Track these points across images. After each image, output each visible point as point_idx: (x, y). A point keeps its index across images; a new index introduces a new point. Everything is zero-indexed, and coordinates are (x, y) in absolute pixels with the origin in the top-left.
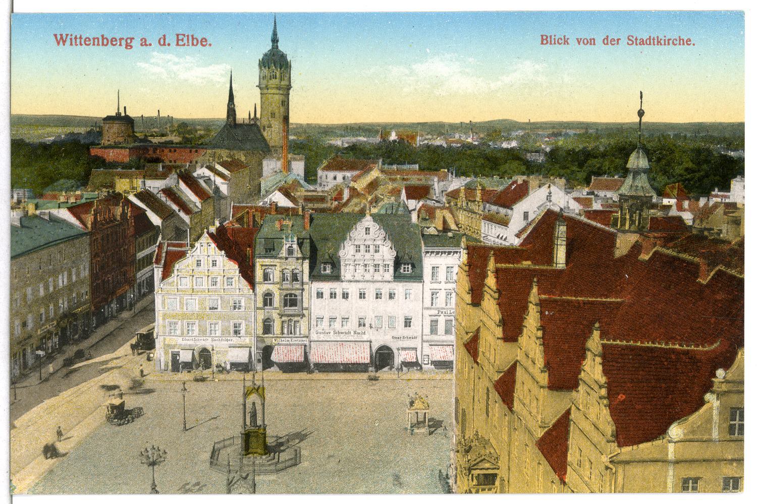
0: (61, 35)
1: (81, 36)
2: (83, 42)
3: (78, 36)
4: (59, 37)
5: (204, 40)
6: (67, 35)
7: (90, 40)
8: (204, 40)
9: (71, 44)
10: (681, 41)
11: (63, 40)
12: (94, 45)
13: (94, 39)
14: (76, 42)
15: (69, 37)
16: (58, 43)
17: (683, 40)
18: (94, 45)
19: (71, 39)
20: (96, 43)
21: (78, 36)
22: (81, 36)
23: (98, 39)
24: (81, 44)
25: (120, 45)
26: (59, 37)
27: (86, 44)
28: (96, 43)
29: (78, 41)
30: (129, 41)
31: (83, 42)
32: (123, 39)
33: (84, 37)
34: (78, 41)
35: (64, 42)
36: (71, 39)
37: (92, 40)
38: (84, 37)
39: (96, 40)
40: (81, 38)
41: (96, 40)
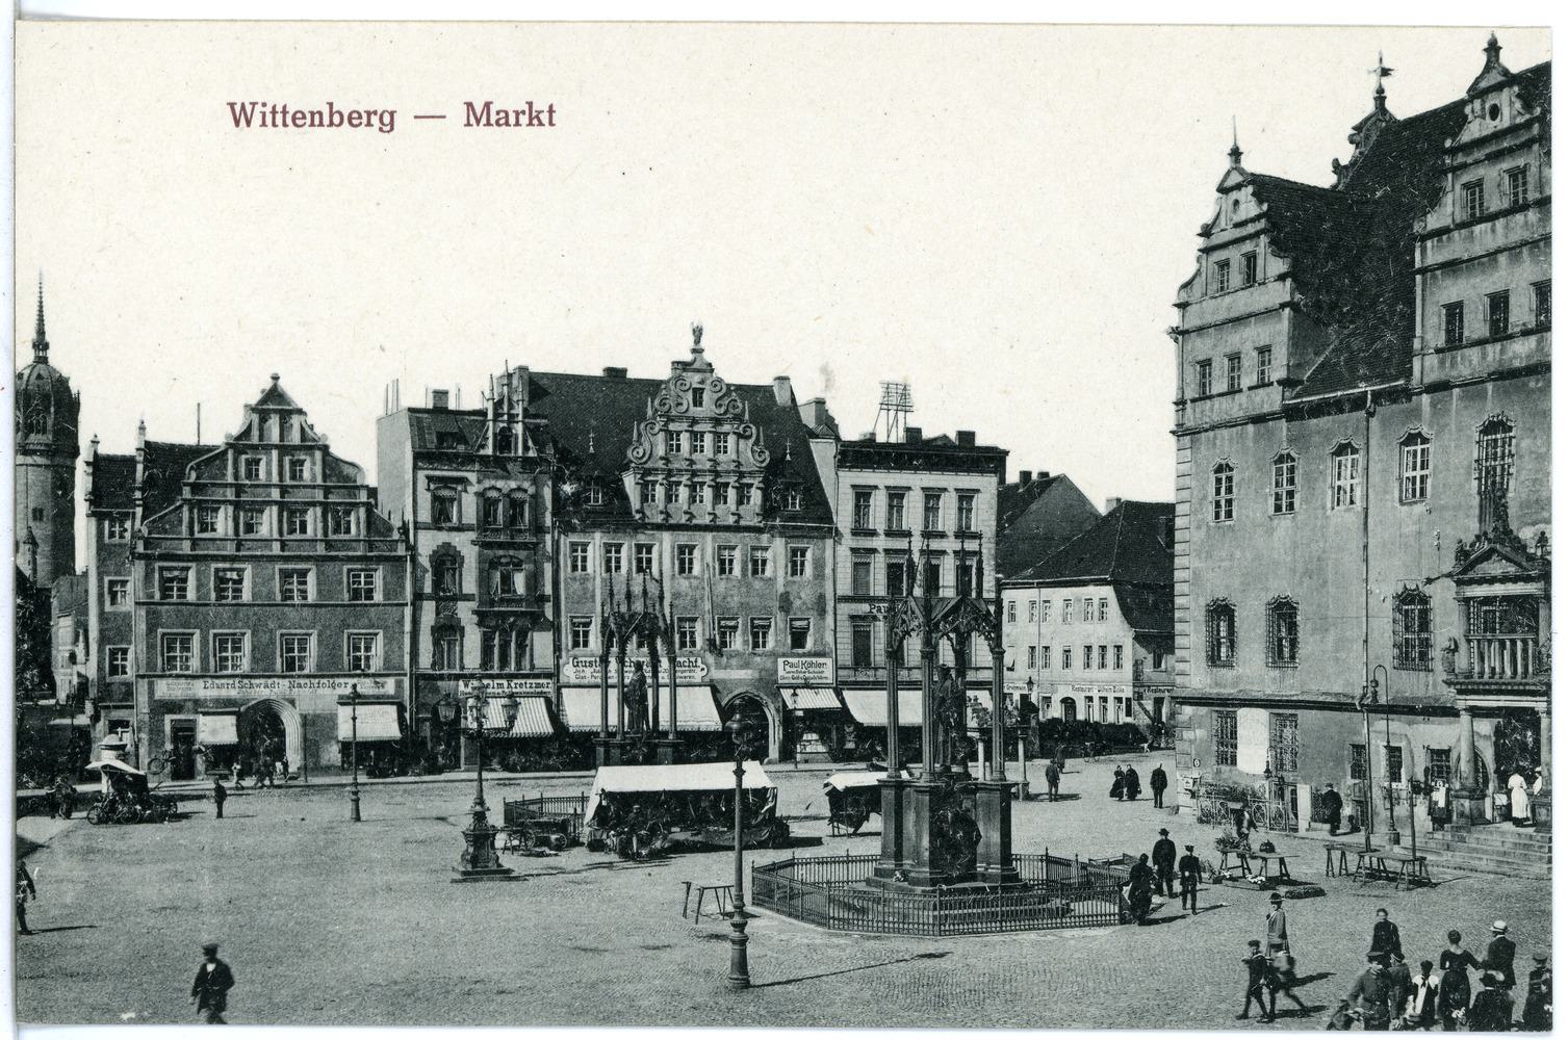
0: (243, 105)
1: (285, 107)
2: (289, 120)
3: (279, 109)
4: (238, 108)
5: (299, 115)
6: (254, 104)
7: (304, 117)
8: (299, 115)
9: (264, 124)
11: (245, 114)
12: (312, 125)
13: (313, 114)
14: (274, 118)
15: (258, 108)
16: (237, 123)
18: (312, 125)
19: (264, 114)
20: (317, 121)
21: (279, 109)
22: (285, 107)
23: (320, 113)
24: (285, 125)
25: (369, 124)
26: (238, 108)
28: (317, 121)
29: (279, 118)
30: (387, 119)
31: (289, 120)
32: (375, 113)
33: (291, 110)
34: (279, 118)
35: (248, 123)
36: (264, 114)
37: (308, 116)
38: (291, 110)
39: (317, 117)
40: (285, 112)
41: (317, 117)
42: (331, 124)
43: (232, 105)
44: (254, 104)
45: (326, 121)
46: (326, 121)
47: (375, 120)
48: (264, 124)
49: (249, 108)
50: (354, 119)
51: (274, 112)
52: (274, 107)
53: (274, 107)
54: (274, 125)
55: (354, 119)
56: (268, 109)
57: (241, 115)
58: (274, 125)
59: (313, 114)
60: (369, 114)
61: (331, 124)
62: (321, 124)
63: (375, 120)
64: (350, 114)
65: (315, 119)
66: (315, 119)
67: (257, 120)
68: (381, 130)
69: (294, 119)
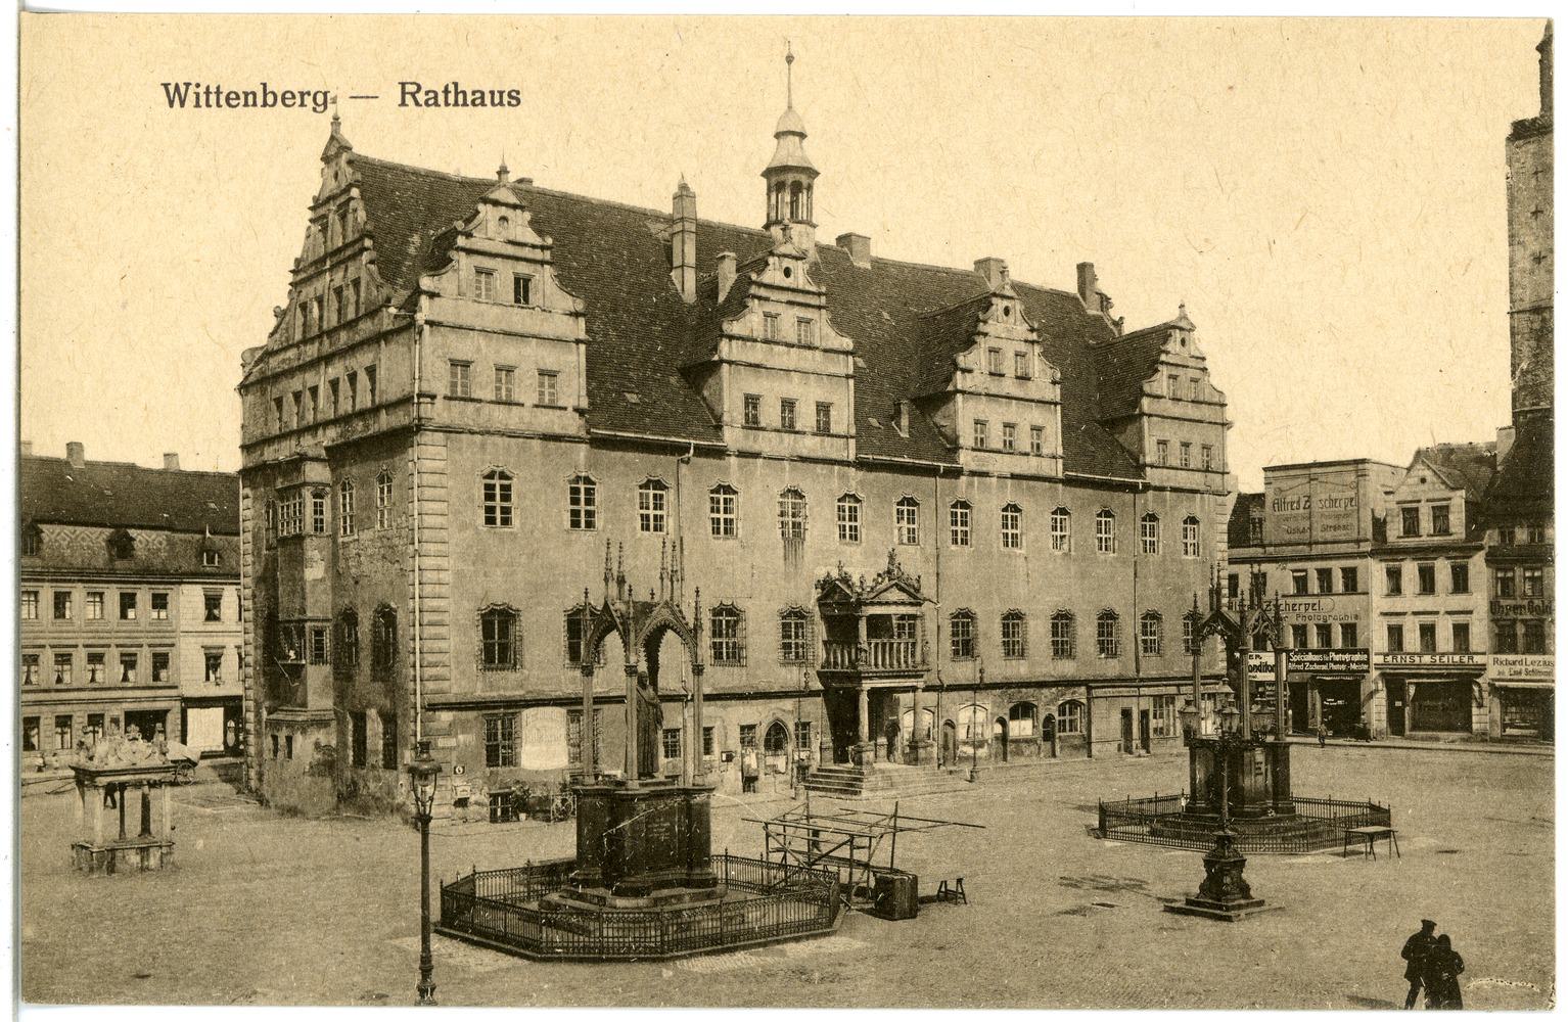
0: (177, 87)
1: (218, 88)
3: (213, 89)
4: (172, 89)
6: (187, 85)
7: (238, 98)
9: (198, 105)
10: (461, 96)
11: (179, 95)
12: (246, 105)
13: (246, 94)
15: (192, 89)
16: (171, 103)
17: (464, 93)
18: (246, 105)
19: (198, 95)
20: (250, 102)
21: (213, 89)
22: (218, 88)
23: (254, 94)
24: (218, 105)
26: (172, 89)
27: (229, 105)
28: (250, 102)
29: (213, 98)
33: (225, 91)
34: (213, 98)
36: (198, 95)
37: (242, 97)
38: (225, 91)
39: (250, 97)
40: (218, 92)
41: (250, 97)
42: (265, 104)
43: (166, 86)
44: (187, 85)
45: (260, 101)
46: (260, 101)
47: (308, 100)
48: (198, 105)
49: (182, 89)
50: (286, 98)
51: (208, 92)
52: (208, 88)
53: (208, 88)
54: (208, 105)
55: (286, 98)
56: (201, 90)
57: (175, 95)
58: (208, 105)
59: (246, 94)
60: (302, 94)
61: (265, 104)
62: (255, 104)
63: (308, 100)
64: (284, 95)
65: (249, 99)
66: (249, 99)
67: (191, 99)
68: (314, 110)
69: (228, 99)
